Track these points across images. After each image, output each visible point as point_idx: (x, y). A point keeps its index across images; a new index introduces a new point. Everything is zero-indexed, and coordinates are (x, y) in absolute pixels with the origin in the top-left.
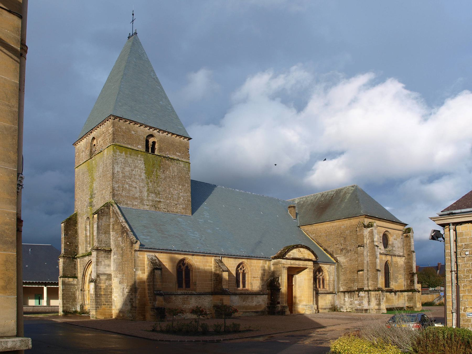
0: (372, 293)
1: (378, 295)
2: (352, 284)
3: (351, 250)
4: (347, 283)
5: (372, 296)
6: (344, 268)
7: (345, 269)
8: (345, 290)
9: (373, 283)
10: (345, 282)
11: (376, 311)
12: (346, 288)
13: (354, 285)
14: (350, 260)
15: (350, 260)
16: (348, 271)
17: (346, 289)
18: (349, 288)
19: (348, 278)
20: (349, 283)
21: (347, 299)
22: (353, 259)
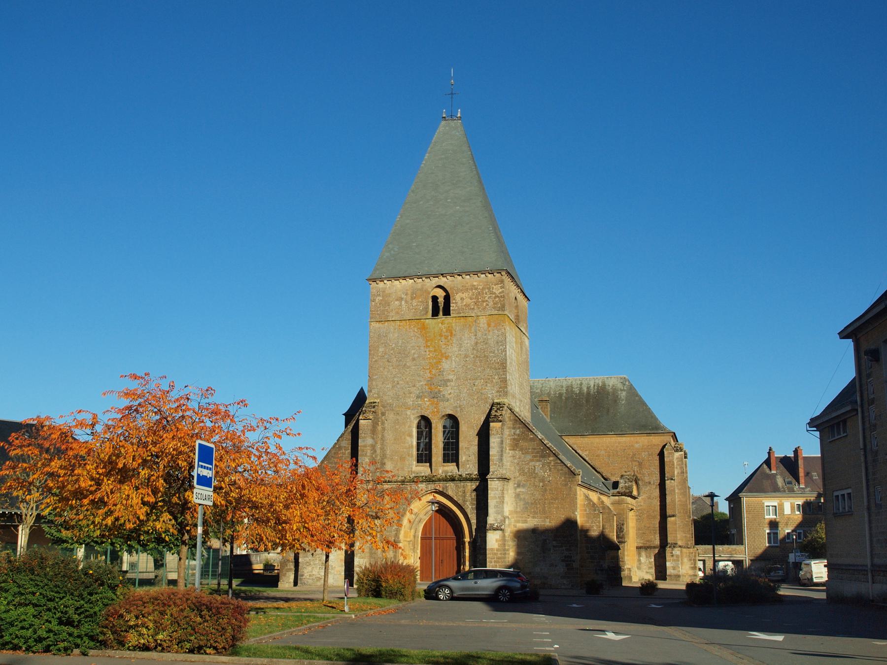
0: (684, 550)
1: (692, 553)
2: (653, 536)
3: (650, 483)
4: (643, 533)
5: (685, 556)
6: (639, 510)
7: (640, 511)
8: (641, 545)
9: (684, 535)
10: (640, 531)
11: (690, 578)
12: (642, 542)
13: (655, 538)
14: (649, 498)
15: (648, 498)
16: (646, 515)
17: (641, 543)
18: (646, 541)
19: (645, 526)
20: (646, 534)
21: (643, 559)
22: (654, 498)
